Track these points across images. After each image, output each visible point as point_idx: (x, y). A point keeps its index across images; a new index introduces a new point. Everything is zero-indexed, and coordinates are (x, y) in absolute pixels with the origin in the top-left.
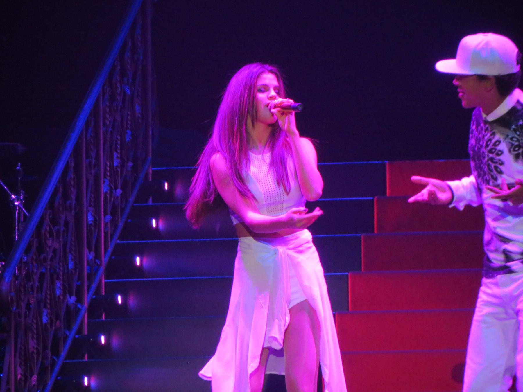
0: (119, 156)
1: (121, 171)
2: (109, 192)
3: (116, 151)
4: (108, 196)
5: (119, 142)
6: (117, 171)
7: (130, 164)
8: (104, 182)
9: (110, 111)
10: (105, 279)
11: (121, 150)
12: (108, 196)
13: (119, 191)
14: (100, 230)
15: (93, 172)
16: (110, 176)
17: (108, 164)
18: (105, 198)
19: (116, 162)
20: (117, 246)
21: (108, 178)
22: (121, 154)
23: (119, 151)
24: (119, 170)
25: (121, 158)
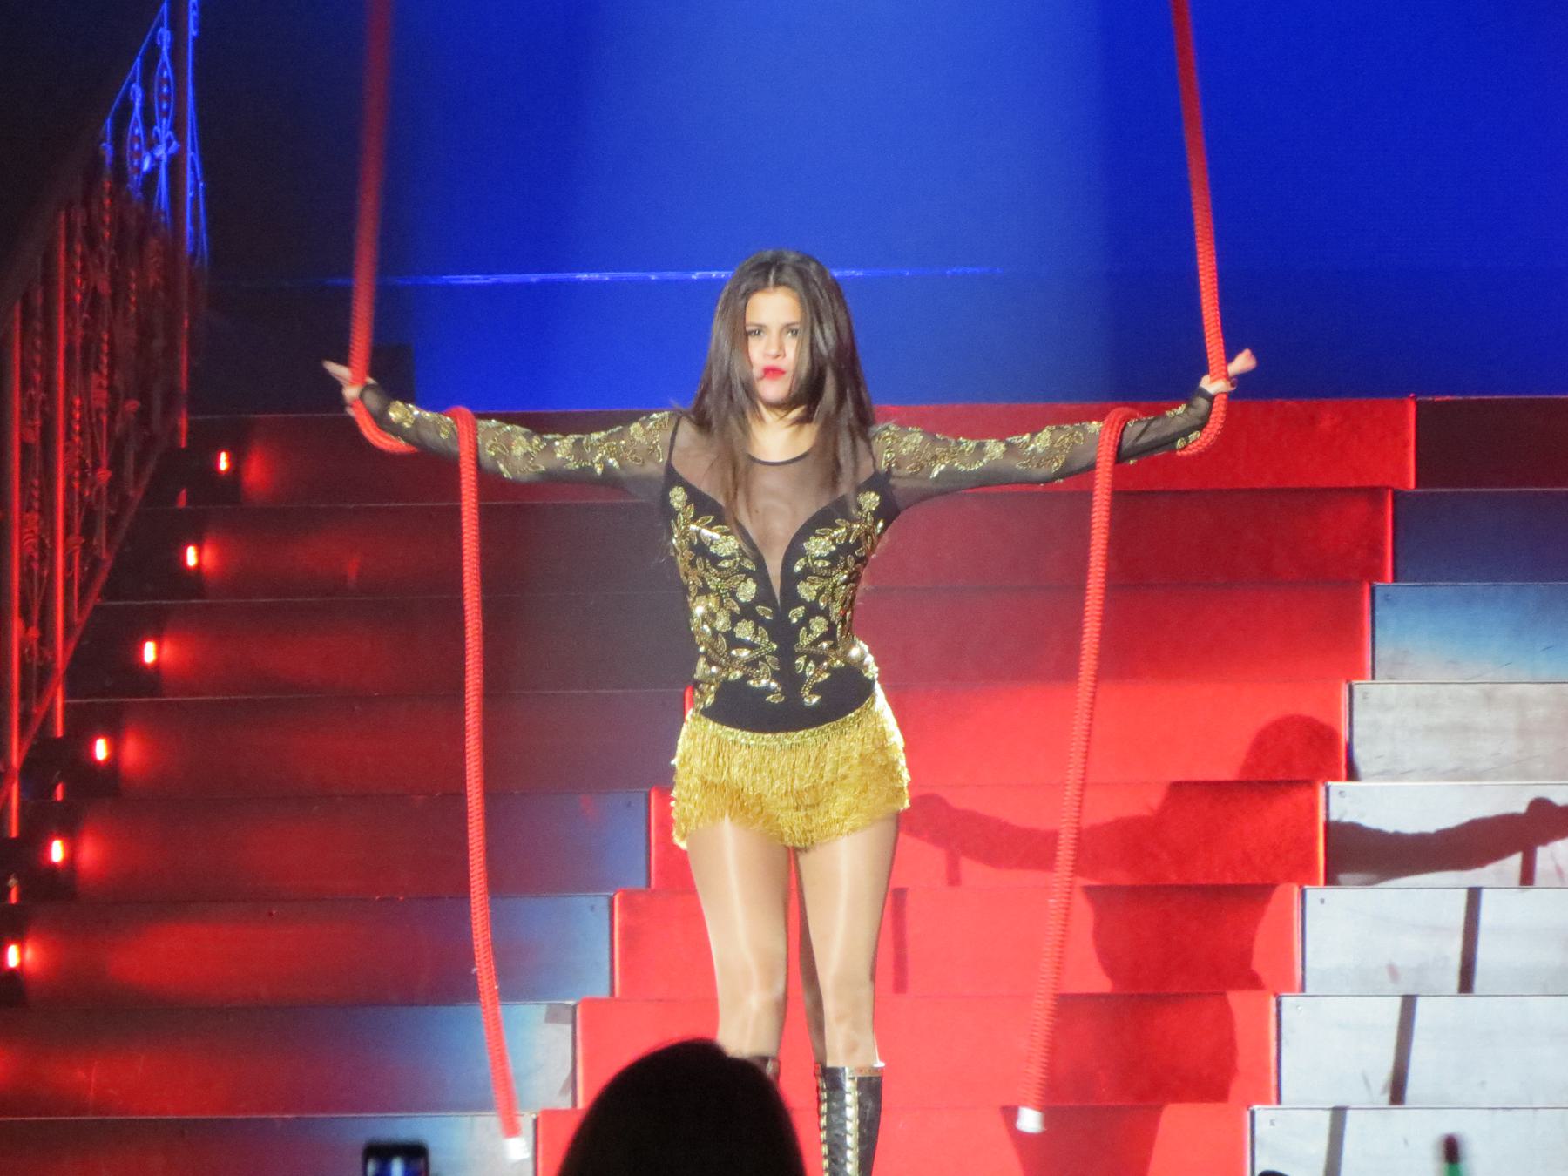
0: (105, 383)
1: (112, 419)
2: (77, 474)
3: (97, 369)
4: (76, 484)
5: (105, 348)
6: (99, 421)
7: (133, 405)
8: (67, 449)
9: (84, 268)
10: (69, 694)
11: (111, 367)
12: (76, 484)
13: (104, 475)
14: (52, 571)
15: (38, 423)
16: (81, 433)
17: (78, 402)
18: (69, 489)
19: (100, 399)
20: (96, 609)
21: (77, 439)
22: (110, 377)
23: (105, 372)
24: (104, 418)
25: (110, 387)
